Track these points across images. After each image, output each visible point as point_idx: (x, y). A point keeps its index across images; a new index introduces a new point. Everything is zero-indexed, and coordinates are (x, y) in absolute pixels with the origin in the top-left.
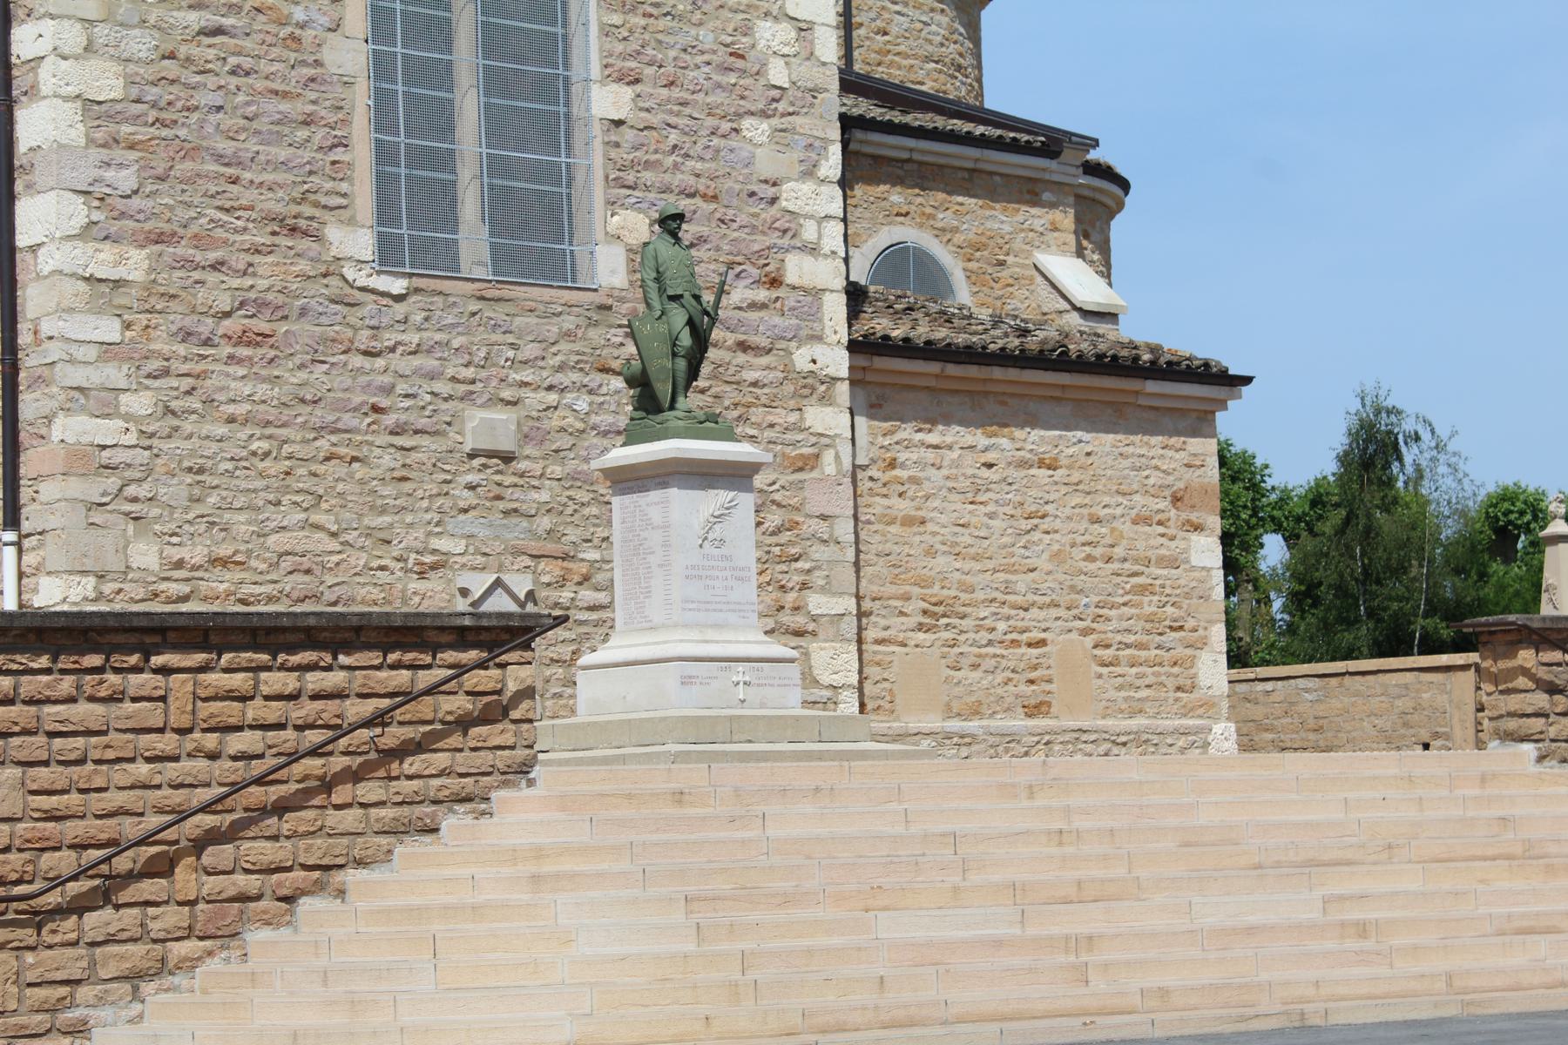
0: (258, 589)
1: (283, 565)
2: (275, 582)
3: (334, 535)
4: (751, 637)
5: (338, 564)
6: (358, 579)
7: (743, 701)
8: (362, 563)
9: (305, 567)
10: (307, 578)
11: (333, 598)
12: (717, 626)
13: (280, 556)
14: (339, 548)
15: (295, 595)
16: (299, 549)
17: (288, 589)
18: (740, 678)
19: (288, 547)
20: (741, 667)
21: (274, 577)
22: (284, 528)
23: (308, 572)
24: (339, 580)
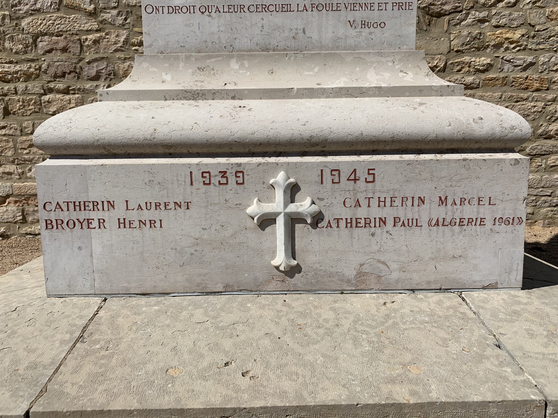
0: (13, 68)
1: (40, 45)
2: (32, 61)
3: (93, 14)
4: (372, 79)
5: (96, 42)
6: (118, 55)
7: (293, 271)
8: (122, 39)
9: (61, 45)
10: (64, 56)
11: (93, 73)
12: (268, 52)
13: (36, 37)
14: (95, 26)
15: (52, 71)
16: (54, 29)
17: (44, 66)
18: (277, 204)
19: (41, 28)
20: (280, 172)
21: (30, 56)
22: (38, 11)
23: (64, 50)
24: (97, 56)
